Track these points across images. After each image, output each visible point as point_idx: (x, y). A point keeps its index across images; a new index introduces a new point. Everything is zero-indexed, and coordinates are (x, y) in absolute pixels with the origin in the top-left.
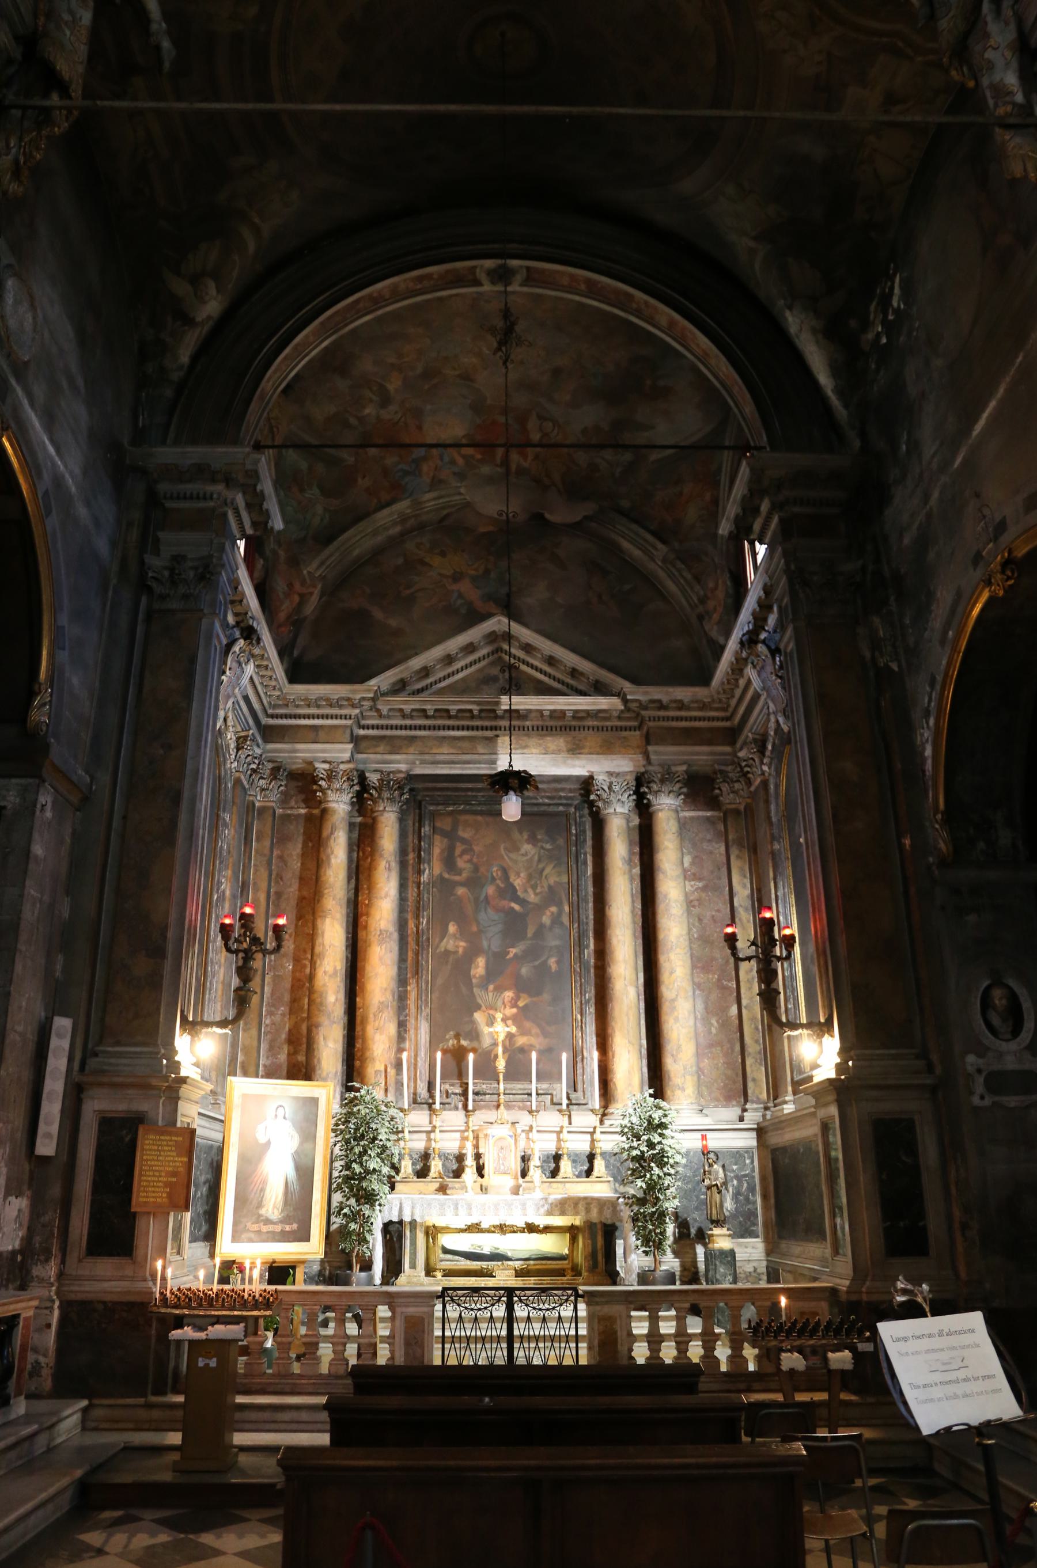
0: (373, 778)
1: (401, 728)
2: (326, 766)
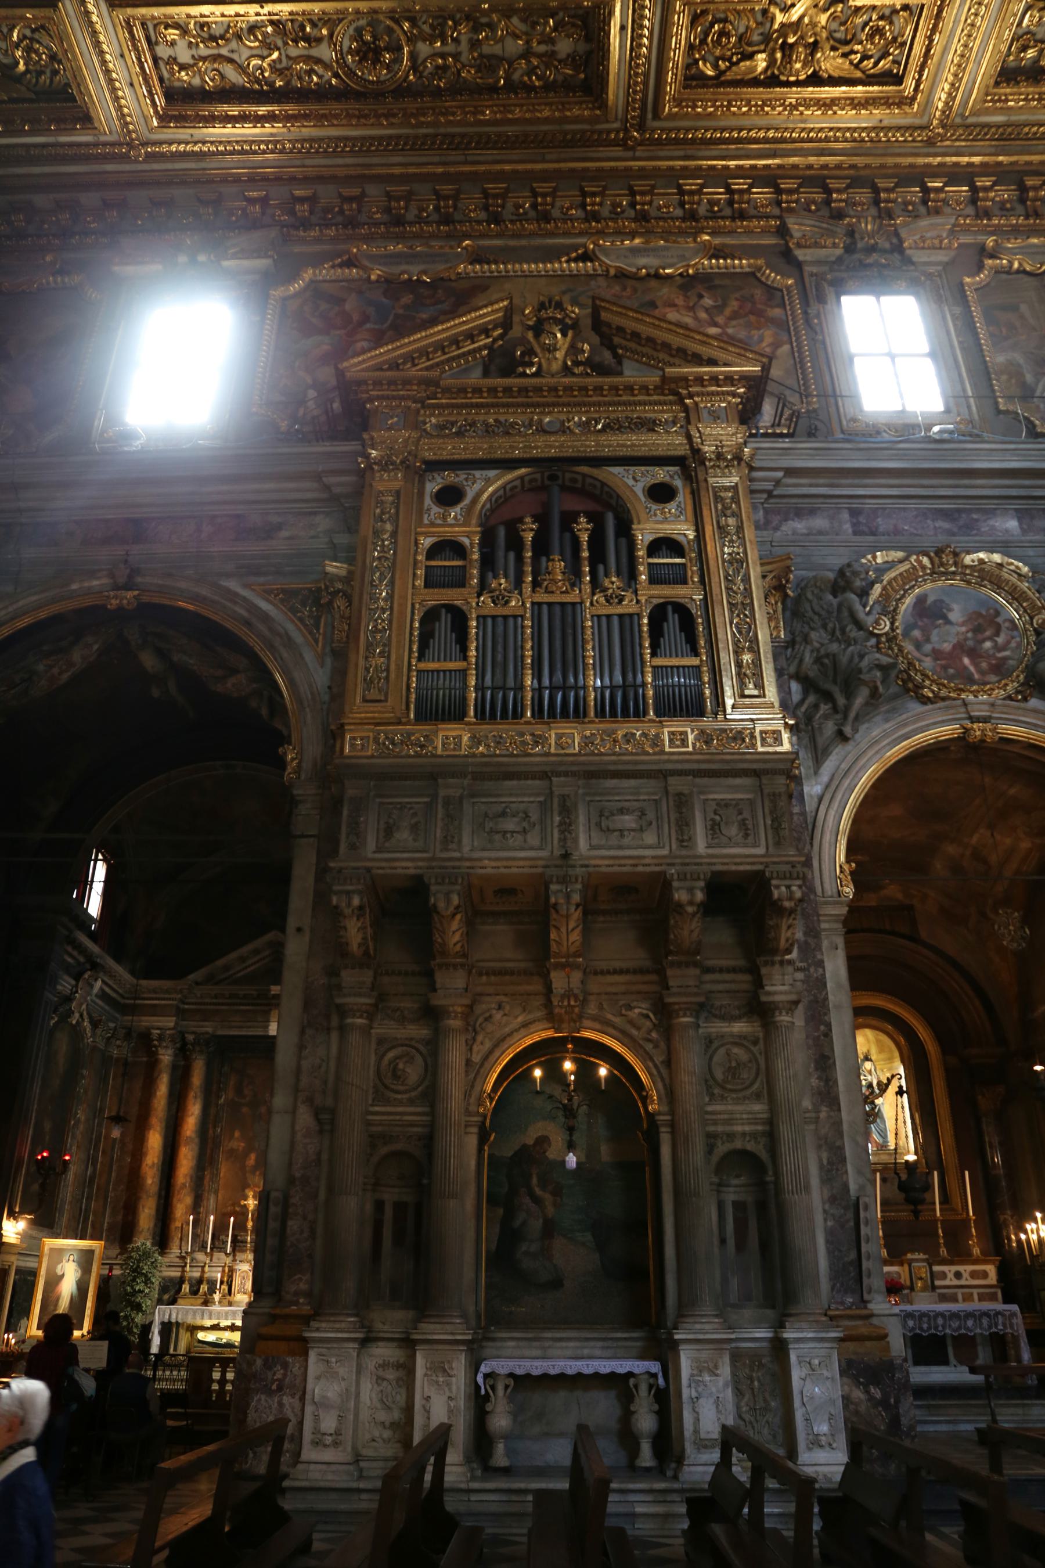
0: (190, 1038)
1: (211, 1004)
2: (158, 1032)
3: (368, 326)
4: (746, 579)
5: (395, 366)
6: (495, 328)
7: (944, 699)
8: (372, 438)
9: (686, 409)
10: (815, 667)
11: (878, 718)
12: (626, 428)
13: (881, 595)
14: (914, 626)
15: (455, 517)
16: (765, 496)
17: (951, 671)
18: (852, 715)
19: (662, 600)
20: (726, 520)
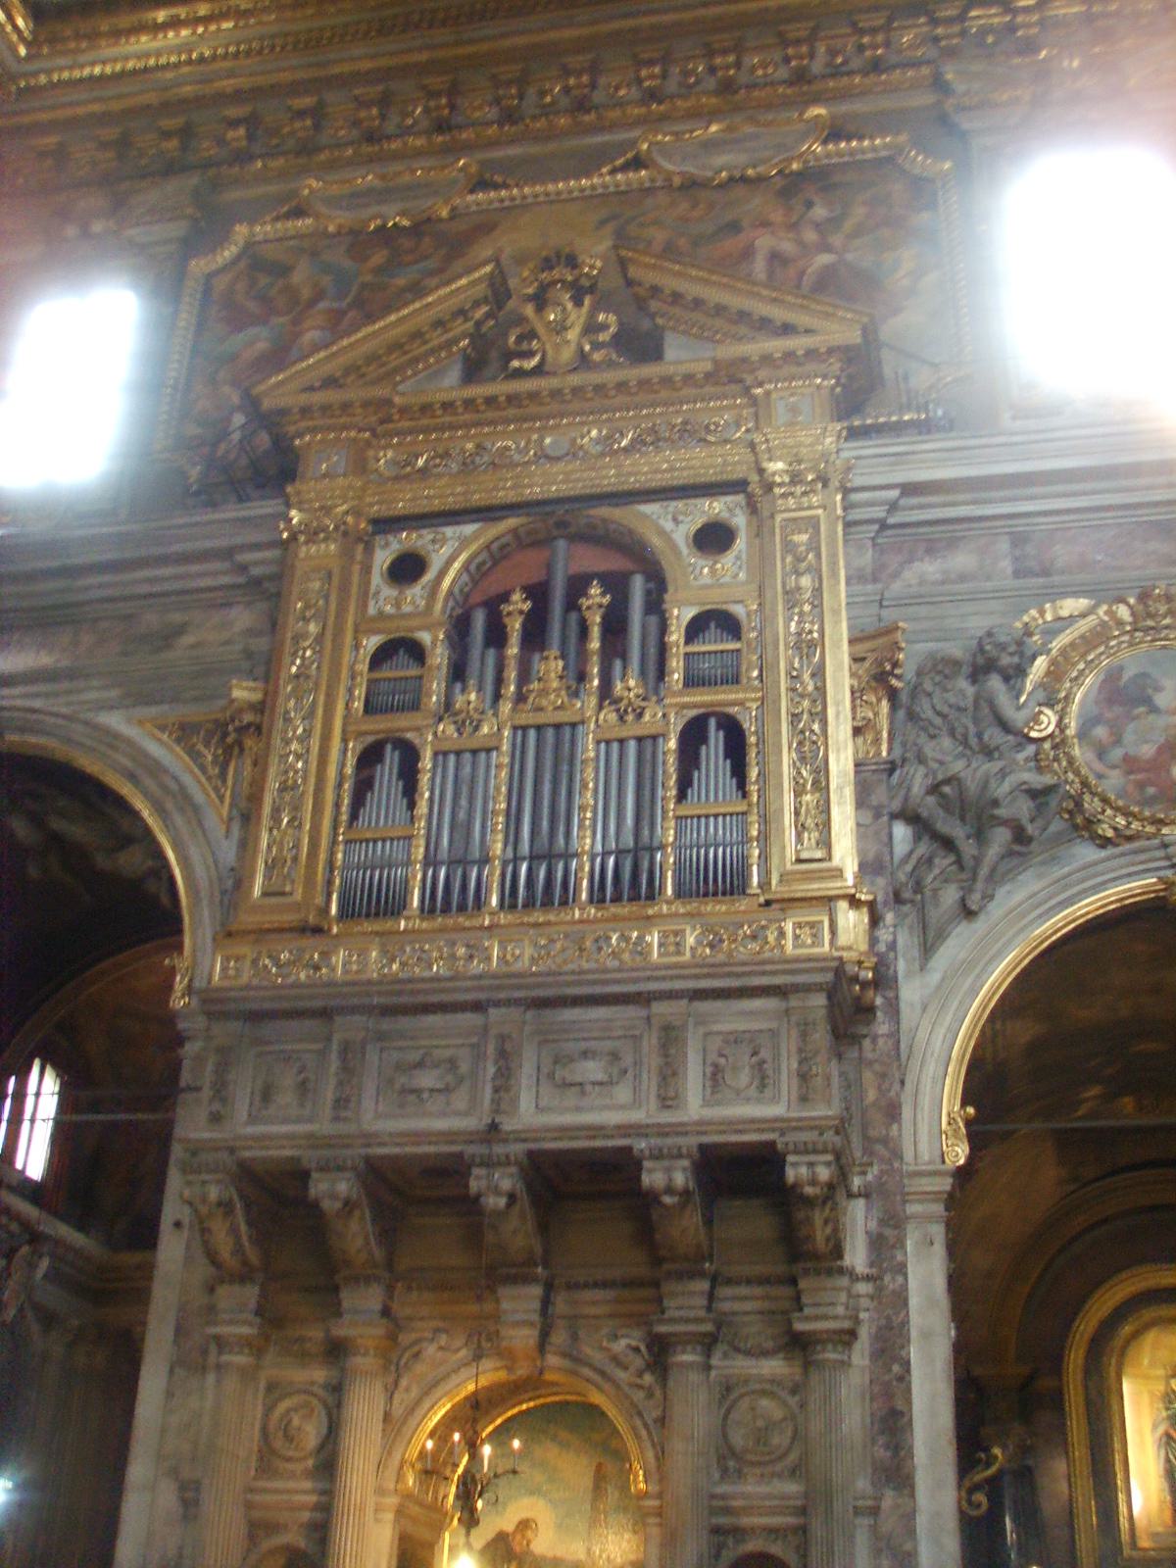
3: (322, 305)
4: (819, 673)
5: (331, 382)
6: (477, 304)
7: (1130, 839)
8: (298, 493)
9: (754, 401)
10: (931, 800)
11: (1029, 873)
12: (666, 440)
13: (1048, 673)
14: (1097, 720)
15: (413, 602)
16: (876, 527)
17: (1151, 790)
18: (984, 871)
19: (702, 711)
20: (796, 580)
